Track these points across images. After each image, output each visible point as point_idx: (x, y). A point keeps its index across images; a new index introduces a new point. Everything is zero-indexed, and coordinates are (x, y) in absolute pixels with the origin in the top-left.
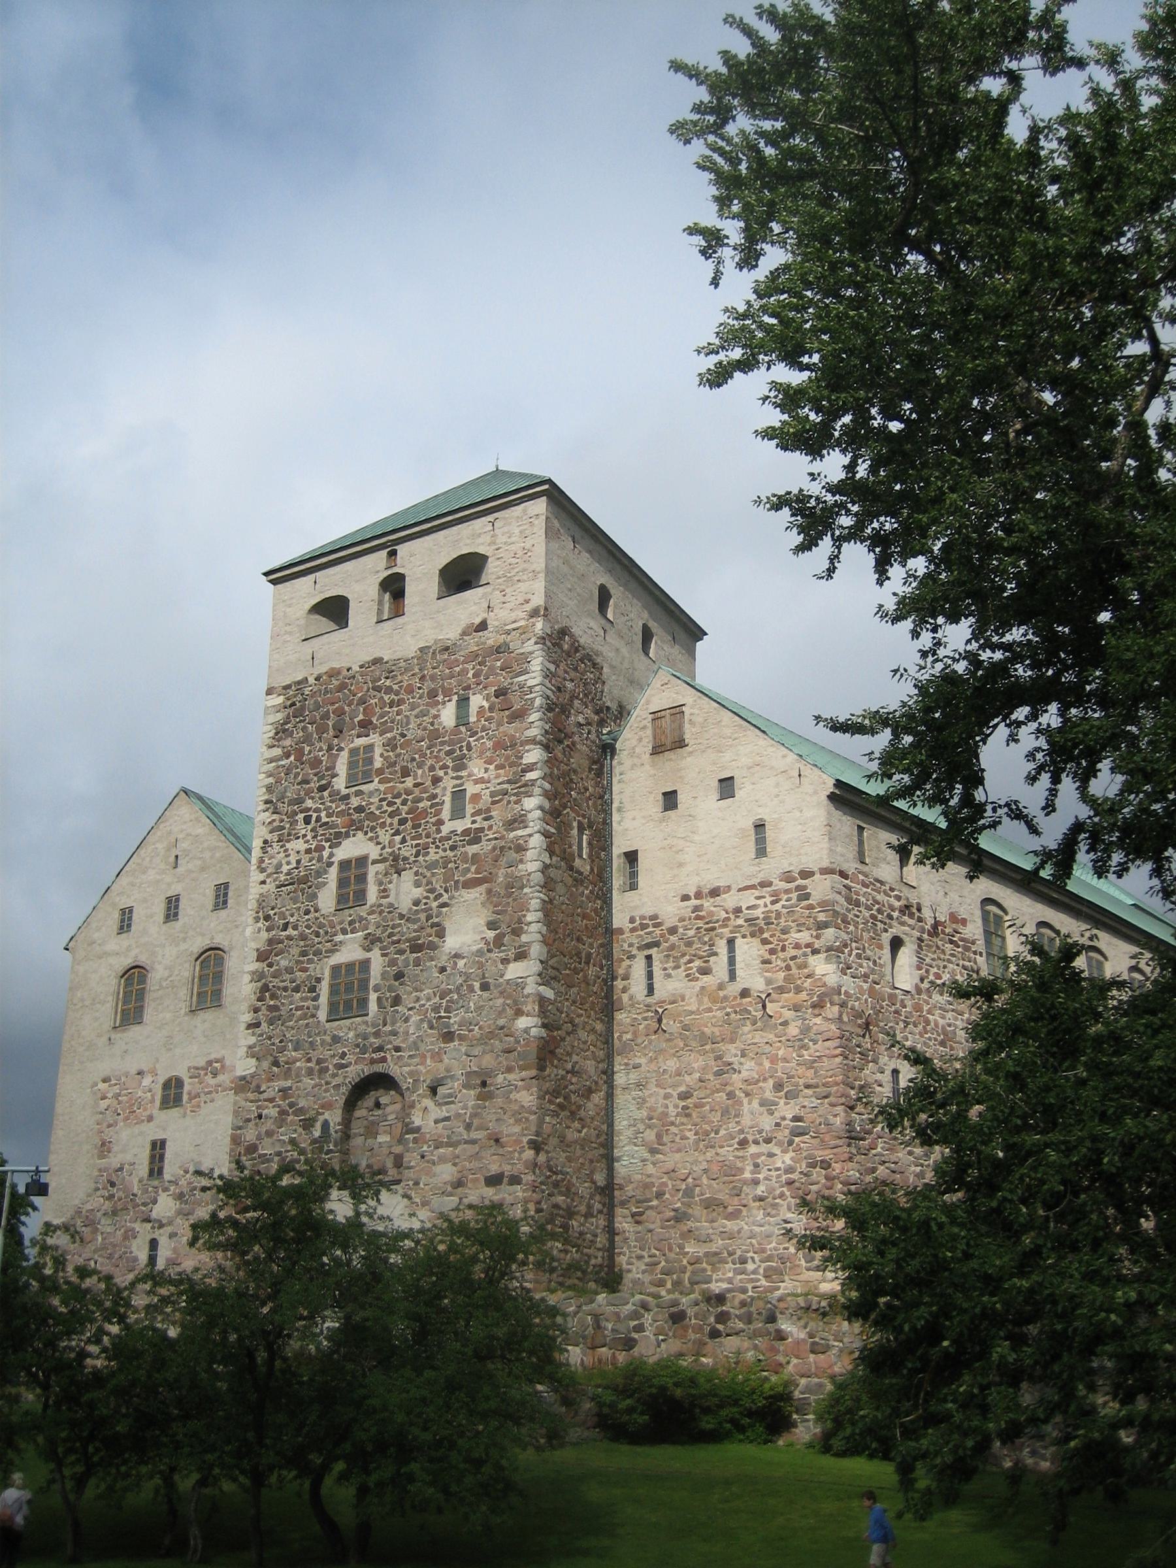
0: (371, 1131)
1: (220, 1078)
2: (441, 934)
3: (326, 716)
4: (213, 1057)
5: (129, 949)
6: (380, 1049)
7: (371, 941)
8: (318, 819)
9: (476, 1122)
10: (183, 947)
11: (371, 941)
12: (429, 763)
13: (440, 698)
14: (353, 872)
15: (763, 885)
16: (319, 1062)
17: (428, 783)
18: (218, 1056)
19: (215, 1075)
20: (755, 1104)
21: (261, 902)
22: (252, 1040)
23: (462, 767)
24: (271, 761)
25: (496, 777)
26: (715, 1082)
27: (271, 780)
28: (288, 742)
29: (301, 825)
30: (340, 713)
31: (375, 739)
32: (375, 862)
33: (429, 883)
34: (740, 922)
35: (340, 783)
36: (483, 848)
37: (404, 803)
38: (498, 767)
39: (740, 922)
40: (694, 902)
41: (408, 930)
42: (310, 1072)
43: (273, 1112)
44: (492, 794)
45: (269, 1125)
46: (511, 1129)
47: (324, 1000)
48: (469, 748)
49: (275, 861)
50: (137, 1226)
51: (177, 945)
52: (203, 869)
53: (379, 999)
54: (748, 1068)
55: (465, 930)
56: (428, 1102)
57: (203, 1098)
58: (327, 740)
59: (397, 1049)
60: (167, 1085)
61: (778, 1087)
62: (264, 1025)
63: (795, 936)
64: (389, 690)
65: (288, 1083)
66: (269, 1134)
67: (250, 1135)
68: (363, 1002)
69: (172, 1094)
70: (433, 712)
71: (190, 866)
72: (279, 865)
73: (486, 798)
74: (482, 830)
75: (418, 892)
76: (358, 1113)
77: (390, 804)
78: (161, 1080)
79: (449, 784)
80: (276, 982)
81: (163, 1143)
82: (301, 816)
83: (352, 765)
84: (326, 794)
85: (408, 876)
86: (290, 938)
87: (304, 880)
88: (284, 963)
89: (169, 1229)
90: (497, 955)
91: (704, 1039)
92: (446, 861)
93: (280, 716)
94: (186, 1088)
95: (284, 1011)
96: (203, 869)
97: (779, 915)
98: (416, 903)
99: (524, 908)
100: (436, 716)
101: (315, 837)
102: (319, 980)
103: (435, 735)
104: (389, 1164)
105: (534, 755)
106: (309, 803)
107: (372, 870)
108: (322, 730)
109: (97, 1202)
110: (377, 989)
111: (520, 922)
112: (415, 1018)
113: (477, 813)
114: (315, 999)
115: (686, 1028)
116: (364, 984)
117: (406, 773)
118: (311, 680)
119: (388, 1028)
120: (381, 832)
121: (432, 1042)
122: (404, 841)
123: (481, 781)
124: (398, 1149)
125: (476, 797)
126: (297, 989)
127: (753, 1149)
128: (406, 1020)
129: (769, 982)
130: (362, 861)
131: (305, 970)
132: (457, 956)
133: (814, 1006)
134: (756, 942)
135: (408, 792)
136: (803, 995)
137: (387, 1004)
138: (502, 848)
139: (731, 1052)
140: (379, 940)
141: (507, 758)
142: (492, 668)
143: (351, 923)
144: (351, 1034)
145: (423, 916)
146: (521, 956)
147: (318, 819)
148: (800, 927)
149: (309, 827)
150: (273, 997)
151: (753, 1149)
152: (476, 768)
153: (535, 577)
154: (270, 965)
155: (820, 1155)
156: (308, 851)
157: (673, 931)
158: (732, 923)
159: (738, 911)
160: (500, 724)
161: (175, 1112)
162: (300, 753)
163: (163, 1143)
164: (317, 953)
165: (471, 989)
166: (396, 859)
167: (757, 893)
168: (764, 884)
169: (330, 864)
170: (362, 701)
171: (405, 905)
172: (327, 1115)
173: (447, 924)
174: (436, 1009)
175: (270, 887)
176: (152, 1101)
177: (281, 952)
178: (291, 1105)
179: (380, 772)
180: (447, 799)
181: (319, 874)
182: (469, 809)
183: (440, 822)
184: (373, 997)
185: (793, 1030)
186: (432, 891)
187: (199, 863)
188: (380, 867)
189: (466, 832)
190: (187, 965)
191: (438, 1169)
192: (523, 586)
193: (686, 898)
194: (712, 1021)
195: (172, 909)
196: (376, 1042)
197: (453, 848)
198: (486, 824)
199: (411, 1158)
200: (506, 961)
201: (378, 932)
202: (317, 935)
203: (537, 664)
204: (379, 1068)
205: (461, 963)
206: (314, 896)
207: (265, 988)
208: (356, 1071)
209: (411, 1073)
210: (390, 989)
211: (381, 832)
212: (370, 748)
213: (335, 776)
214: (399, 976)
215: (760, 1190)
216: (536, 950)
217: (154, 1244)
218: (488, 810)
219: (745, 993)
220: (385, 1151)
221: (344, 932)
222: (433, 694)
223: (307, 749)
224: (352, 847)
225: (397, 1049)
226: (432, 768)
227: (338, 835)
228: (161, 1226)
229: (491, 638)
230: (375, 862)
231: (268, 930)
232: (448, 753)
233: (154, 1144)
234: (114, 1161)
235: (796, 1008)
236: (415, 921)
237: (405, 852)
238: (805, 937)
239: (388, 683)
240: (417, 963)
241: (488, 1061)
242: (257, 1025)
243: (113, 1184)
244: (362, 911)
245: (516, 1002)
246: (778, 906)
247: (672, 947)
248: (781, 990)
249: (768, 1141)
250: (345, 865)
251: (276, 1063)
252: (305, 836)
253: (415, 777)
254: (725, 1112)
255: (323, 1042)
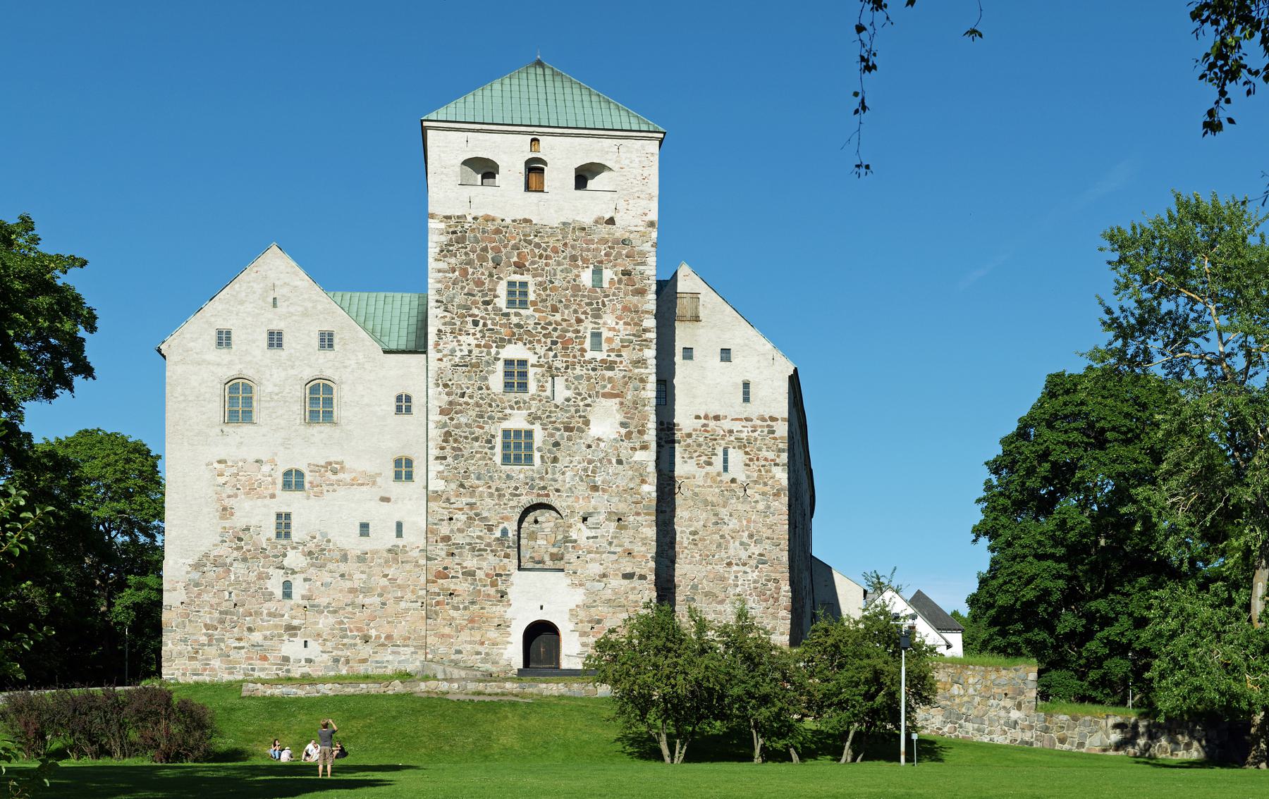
0: (533, 536)
1: (340, 476)
2: (587, 423)
3: (485, 249)
4: (332, 459)
5: (231, 363)
6: (544, 488)
7: (533, 418)
8: (485, 325)
9: (615, 541)
10: (291, 372)
11: (533, 418)
12: (574, 307)
13: (580, 263)
14: (516, 369)
15: (747, 419)
16: (497, 490)
17: (573, 321)
18: (339, 460)
19: (335, 473)
20: (737, 543)
21: (441, 372)
22: (441, 468)
23: (599, 317)
24: (439, 271)
25: (624, 331)
26: (711, 528)
27: (439, 286)
28: (453, 260)
29: (470, 325)
30: (497, 250)
31: (526, 278)
32: (533, 366)
33: (576, 388)
34: (732, 438)
35: (502, 302)
36: (616, 374)
37: (555, 330)
38: (625, 323)
39: (732, 438)
40: (703, 421)
41: (561, 417)
42: (491, 495)
43: (464, 518)
44: (622, 341)
45: (459, 525)
46: (638, 548)
47: (498, 449)
48: (604, 305)
49: (450, 347)
50: (271, 571)
51: (285, 370)
52: (305, 314)
53: (542, 457)
54: (733, 524)
55: (605, 423)
56: (581, 525)
57: (325, 488)
58: (487, 268)
59: (558, 491)
60: (287, 474)
61: (751, 536)
62: (450, 460)
63: (764, 453)
64: (538, 246)
65: (473, 501)
66: (460, 531)
67: (445, 530)
68: (529, 459)
69: (293, 480)
70: (575, 271)
71: (292, 309)
72: (453, 351)
73: (617, 342)
74: (615, 362)
75: (569, 394)
76: (525, 525)
77: (543, 328)
78: (283, 468)
79: (588, 327)
80: (457, 431)
81: (288, 516)
82: (470, 319)
83: (511, 293)
84: (490, 307)
85: (560, 382)
86: (467, 404)
87: (477, 365)
88: (463, 420)
89: (303, 576)
90: (625, 444)
91: (706, 503)
92: (589, 378)
93: (444, 239)
94: (308, 478)
95: (466, 453)
96: (305, 314)
97: (756, 439)
98: (568, 400)
99: (645, 418)
100: (578, 276)
101: (483, 337)
102: (493, 436)
103: (577, 288)
104: (547, 558)
105: (650, 322)
106: (475, 311)
107: (531, 372)
108: (482, 259)
109: (223, 550)
110: (539, 450)
111: (643, 426)
112: (568, 474)
113: (612, 350)
114: (492, 448)
115: (696, 494)
116: (529, 446)
117: (555, 309)
118: (469, 219)
119: (549, 476)
120: (538, 347)
121: (582, 489)
122: (555, 356)
123: (614, 329)
124: (555, 550)
125: (609, 340)
126: (476, 439)
127: (735, 568)
128: (563, 473)
129: (748, 477)
130: (523, 363)
131: (482, 428)
132: (599, 439)
133: (774, 495)
134: (741, 452)
135: (556, 323)
136: (768, 488)
137: (549, 461)
138: (630, 378)
139: (723, 512)
140: (540, 418)
141: (632, 319)
142: (619, 254)
143: (516, 403)
144: (522, 476)
145: (573, 409)
146: (644, 447)
147: (485, 325)
148: (768, 449)
149: (478, 329)
150: (456, 441)
151: (735, 568)
152: (609, 319)
153: (651, 198)
154: (452, 419)
155: (773, 576)
156: (478, 346)
157: (689, 435)
158: (727, 439)
159: (731, 432)
160: (626, 294)
161: (298, 494)
162: (464, 273)
163: (288, 516)
164: (490, 418)
165: (610, 462)
166: (550, 367)
167: (744, 423)
168: (747, 419)
169: (497, 359)
170: (516, 247)
171: (559, 399)
172: (506, 524)
173: (590, 417)
174: (585, 470)
175: (446, 364)
176: (274, 483)
177: (461, 412)
178: (477, 515)
179: (534, 303)
180: (588, 335)
181: (488, 363)
182: (605, 346)
183: (583, 350)
184: (537, 455)
185: (761, 506)
186: (580, 394)
187: (300, 309)
188: (539, 370)
189: (603, 361)
190: (298, 387)
191: (590, 566)
192: (643, 203)
193: (698, 417)
194: (712, 494)
195: (275, 340)
196: (542, 484)
197: (594, 370)
198: (618, 359)
199: (570, 556)
200: (634, 449)
201: (539, 413)
202: (490, 406)
203: (652, 260)
204: (545, 500)
205: (602, 445)
206: (486, 378)
207: (448, 434)
208: (526, 500)
209: (568, 507)
210: (550, 451)
211: (538, 347)
212: (524, 284)
213: (496, 296)
214: (556, 444)
215: (738, 590)
216: (653, 446)
217: (287, 586)
218: (619, 350)
219: (733, 481)
220: (543, 550)
221: (512, 408)
222: (574, 258)
223: (471, 271)
224: (514, 351)
225: (558, 491)
226: (575, 311)
227: (502, 340)
228: (294, 572)
229: (618, 232)
230: (533, 366)
231: (448, 394)
232: (587, 304)
233: (279, 516)
234: (239, 521)
235: (764, 494)
236: (567, 411)
237: (558, 364)
238: (771, 455)
239: (537, 240)
240: (569, 439)
241: (622, 507)
242: (445, 458)
243: (240, 539)
244: (526, 397)
245: (641, 475)
246: (756, 434)
247: (689, 445)
248: (756, 482)
249: (745, 564)
250: (509, 363)
251: (462, 486)
252: (474, 334)
253: (563, 313)
254: (719, 545)
255: (500, 478)
